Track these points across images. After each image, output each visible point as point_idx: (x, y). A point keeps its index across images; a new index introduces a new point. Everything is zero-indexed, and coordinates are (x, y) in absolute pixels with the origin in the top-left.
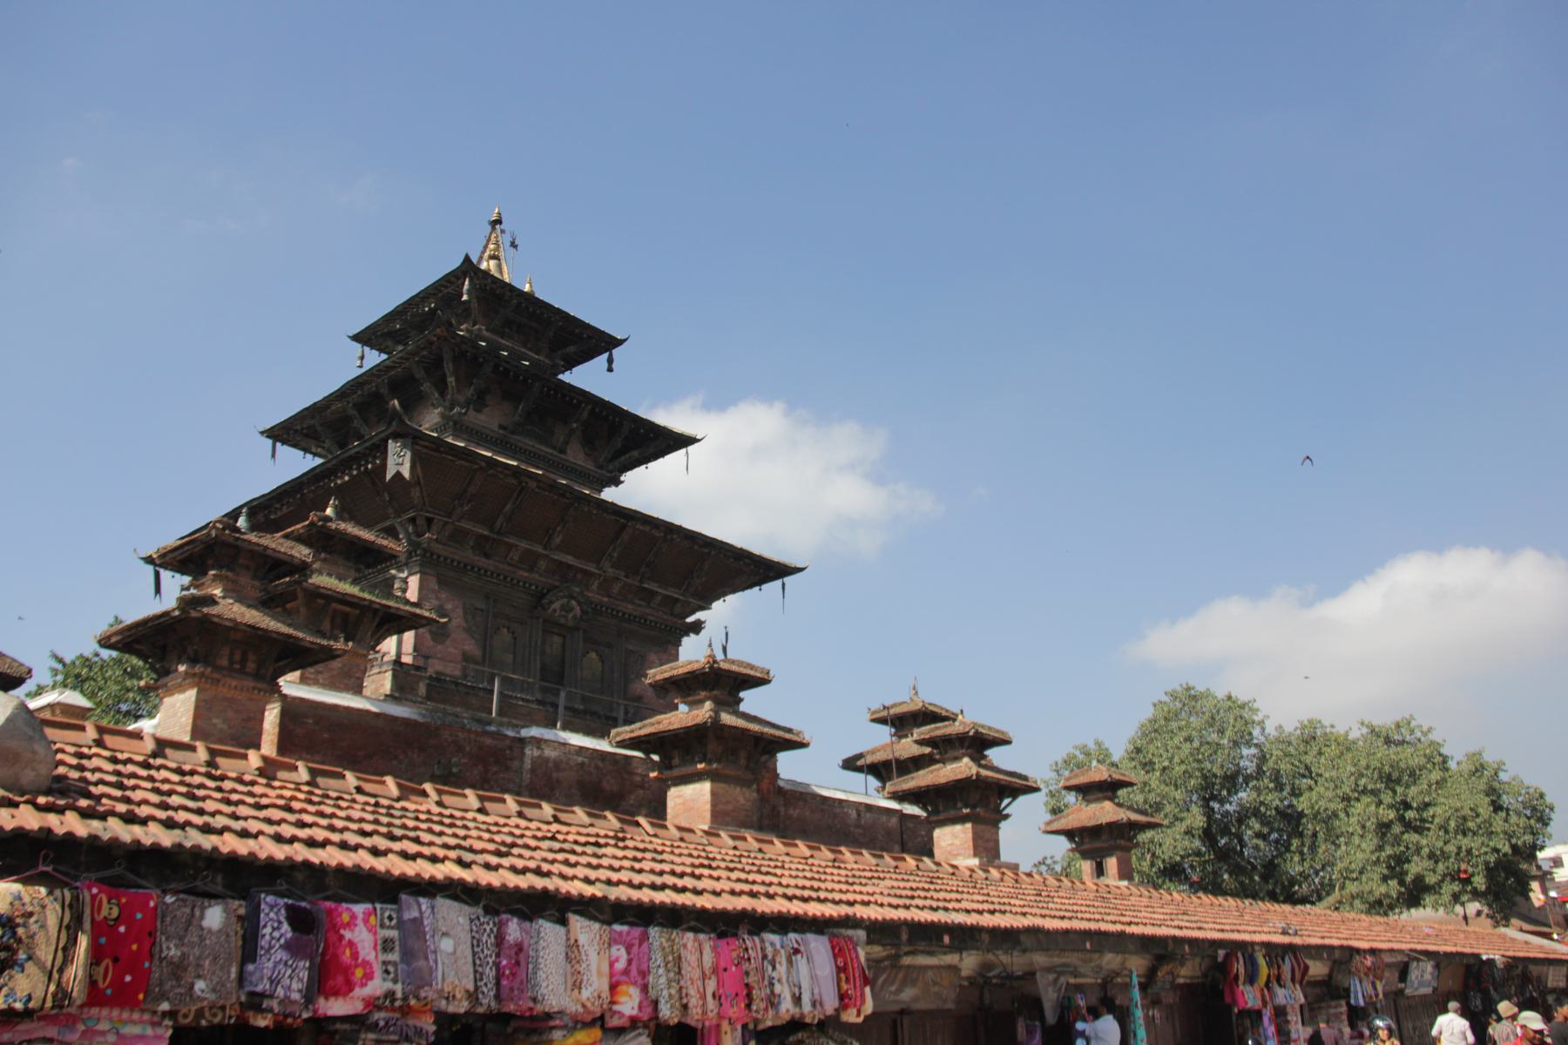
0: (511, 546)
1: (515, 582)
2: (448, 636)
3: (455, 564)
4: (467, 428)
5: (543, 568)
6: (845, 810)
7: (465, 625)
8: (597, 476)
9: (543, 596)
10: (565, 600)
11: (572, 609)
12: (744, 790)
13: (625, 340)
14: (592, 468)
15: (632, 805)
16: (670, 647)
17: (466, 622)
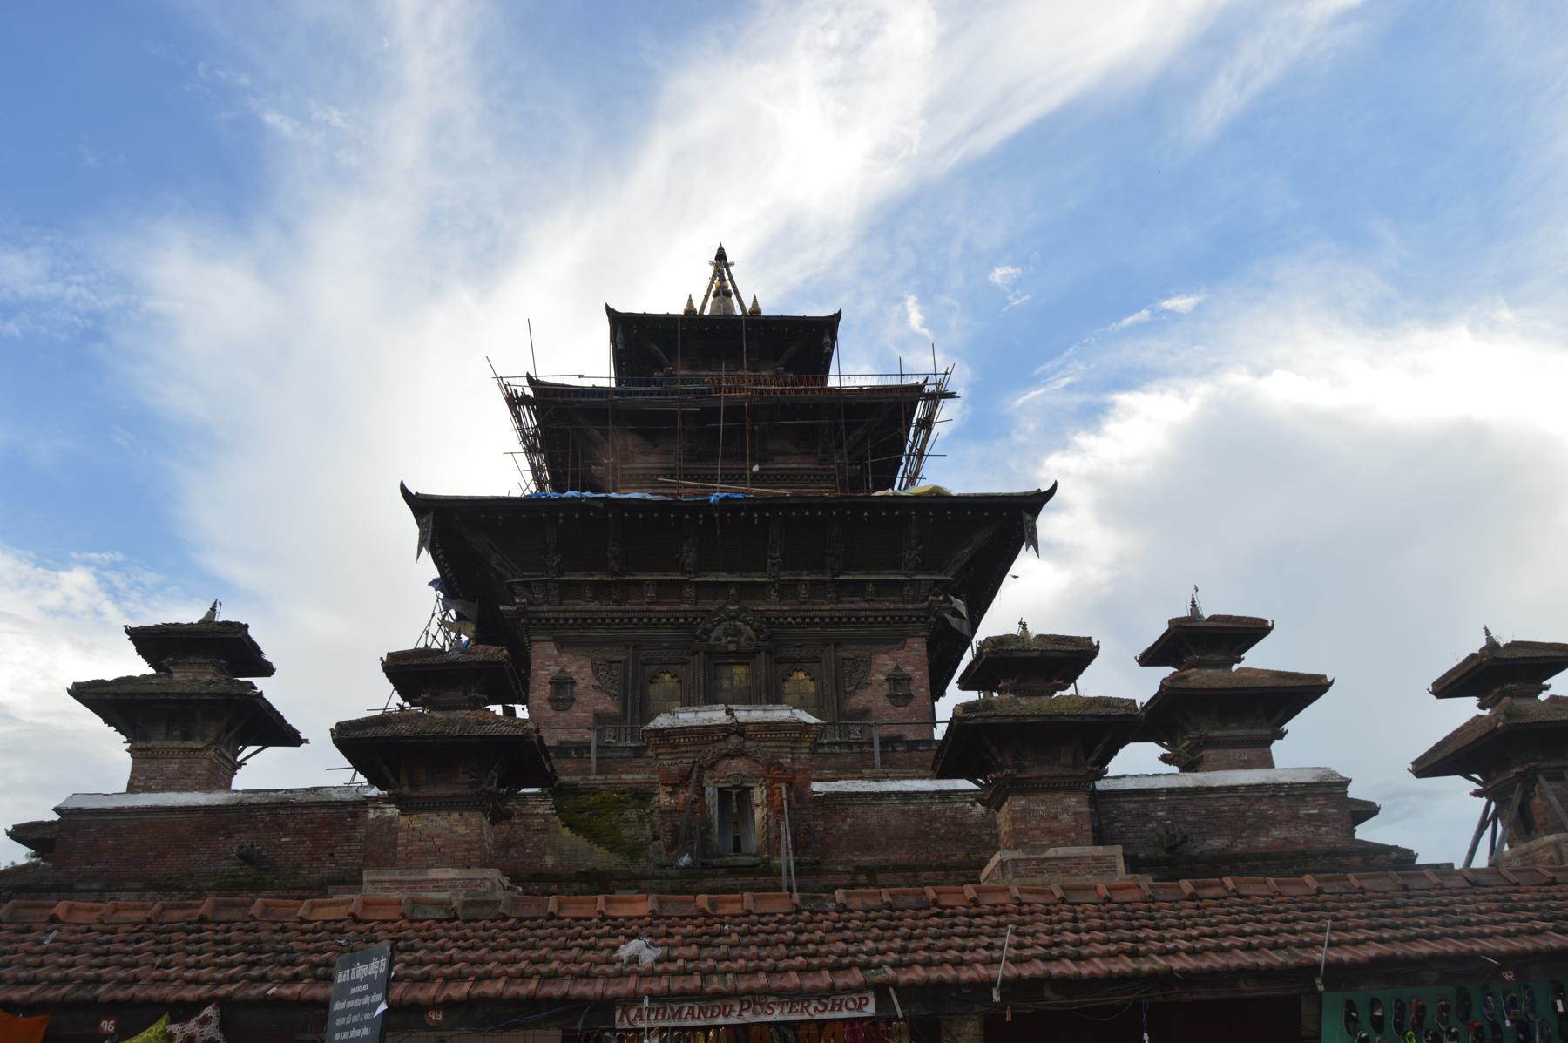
0: (639, 584)
1: (654, 620)
2: (573, 700)
3: (571, 621)
4: (631, 476)
5: (693, 594)
6: (958, 805)
7: (597, 683)
8: (819, 472)
9: (699, 624)
10: (727, 623)
11: (738, 632)
12: (466, 814)
13: (838, 316)
14: (814, 466)
15: (529, 856)
16: (909, 640)
17: (598, 679)
